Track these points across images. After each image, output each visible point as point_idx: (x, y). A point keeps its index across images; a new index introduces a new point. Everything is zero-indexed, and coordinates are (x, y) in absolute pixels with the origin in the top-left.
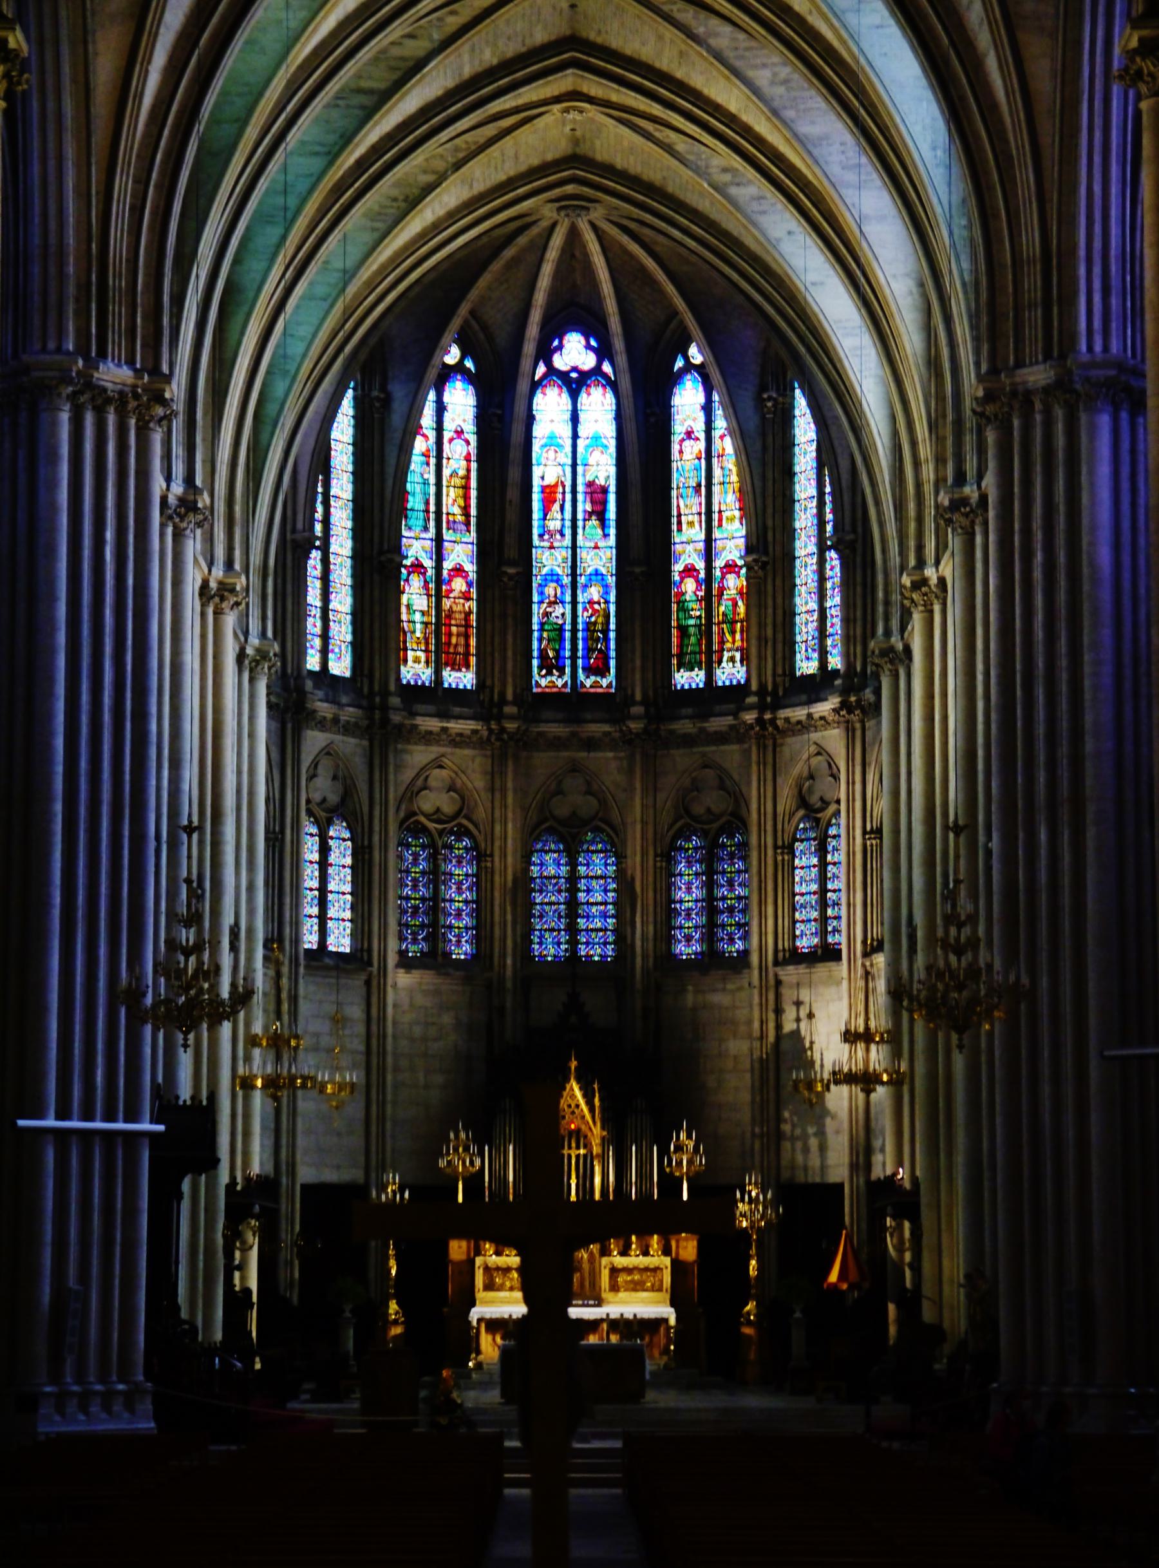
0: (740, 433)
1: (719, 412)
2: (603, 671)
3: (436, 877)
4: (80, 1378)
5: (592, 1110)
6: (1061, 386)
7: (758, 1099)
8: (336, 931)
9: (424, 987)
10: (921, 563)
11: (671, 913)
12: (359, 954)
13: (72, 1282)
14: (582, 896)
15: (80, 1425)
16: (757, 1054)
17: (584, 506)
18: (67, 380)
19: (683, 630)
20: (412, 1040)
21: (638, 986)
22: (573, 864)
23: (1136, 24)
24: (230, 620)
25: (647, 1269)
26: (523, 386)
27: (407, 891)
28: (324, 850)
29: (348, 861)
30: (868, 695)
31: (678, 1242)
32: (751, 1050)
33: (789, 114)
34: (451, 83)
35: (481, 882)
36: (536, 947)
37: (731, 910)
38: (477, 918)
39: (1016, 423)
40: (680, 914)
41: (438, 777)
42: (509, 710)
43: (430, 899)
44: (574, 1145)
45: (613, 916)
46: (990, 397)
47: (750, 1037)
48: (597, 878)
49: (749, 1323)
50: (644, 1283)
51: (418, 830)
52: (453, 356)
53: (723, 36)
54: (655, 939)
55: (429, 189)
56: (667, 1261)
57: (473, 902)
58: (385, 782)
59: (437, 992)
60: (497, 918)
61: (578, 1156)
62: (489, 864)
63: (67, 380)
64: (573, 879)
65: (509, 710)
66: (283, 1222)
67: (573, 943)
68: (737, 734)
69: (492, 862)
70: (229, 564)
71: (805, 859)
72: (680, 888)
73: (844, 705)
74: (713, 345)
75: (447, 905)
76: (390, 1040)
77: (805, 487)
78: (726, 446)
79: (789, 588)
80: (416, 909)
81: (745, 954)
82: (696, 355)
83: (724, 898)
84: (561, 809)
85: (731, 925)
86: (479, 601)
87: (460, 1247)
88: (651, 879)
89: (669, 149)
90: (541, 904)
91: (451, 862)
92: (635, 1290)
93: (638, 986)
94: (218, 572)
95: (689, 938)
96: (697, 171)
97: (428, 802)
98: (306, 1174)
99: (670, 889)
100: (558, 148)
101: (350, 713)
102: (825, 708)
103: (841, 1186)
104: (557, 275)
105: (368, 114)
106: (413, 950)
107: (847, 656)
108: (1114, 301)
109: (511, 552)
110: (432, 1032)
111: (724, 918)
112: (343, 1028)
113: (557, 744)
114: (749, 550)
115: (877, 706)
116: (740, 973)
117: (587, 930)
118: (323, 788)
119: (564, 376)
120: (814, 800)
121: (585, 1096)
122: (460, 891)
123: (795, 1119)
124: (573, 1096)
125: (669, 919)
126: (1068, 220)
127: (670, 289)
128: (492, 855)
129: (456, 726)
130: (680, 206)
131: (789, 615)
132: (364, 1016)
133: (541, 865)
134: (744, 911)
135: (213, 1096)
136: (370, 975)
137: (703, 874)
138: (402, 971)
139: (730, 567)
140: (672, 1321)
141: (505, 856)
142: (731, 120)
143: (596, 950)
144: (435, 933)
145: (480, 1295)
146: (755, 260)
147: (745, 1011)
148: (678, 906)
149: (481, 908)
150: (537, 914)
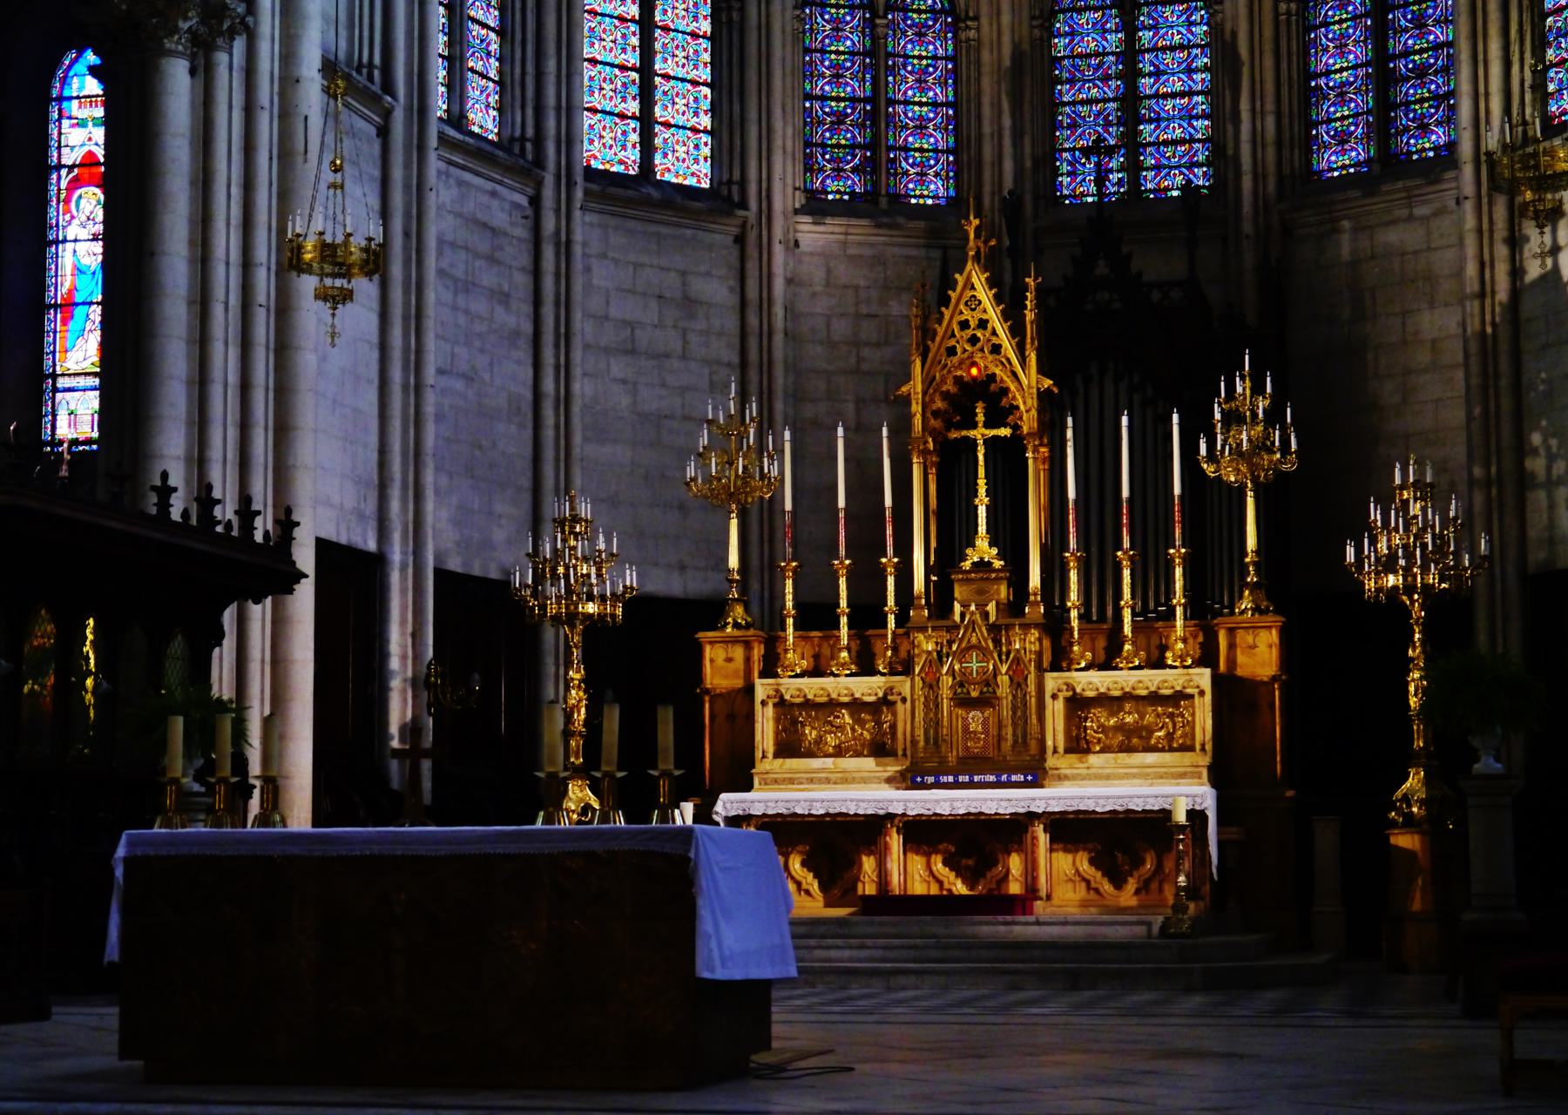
5: (1017, 331)
7: (1477, 411)
8: (681, 149)
9: (851, 251)
12: (725, 192)
14: (1146, 83)
16: (1473, 325)
20: (832, 345)
21: (1247, 227)
22: (1130, 29)
25: (1155, 698)
27: (822, 86)
29: (705, 26)
31: (1231, 632)
32: (1463, 325)
35: (961, 69)
36: (1066, 180)
37: (1421, 72)
38: (957, 133)
40: (1326, 97)
43: (865, 100)
44: (981, 418)
45: (1204, 116)
47: (1461, 303)
48: (1172, 49)
49: (1410, 823)
50: (1151, 732)
54: (1279, 143)
56: (1203, 677)
57: (947, 104)
59: (878, 261)
60: (987, 129)
61: (990, 443)
62: (972, 34)
64: (1130, 54)
66: (549, 661)
69: (978, 29)
72: (1326, 50)
75: (900, 109)
76: (779, 339)
80: (840, 117)
81: (1451, 146)
83: (1407, 53)
85: (1421, 101)
87: (729, 660)
88: (1268, 32)
90: (1073, 103)
91: (904, 33)
92: (1127, 748)
93: (1247, 227)
95: (1342, 138)
99: (1307, 54)
110: (869, 331)
111: (1408, 90)
112: (692, 316)
116: (1438, 181)
117: (1156, 144)
121: (998, 299)
122: (921, 84)
123: (1554, 442)
124: (974, 303)
125: (1307, 106)
128: (976, 18)
132: (734, 300)
133: (1072, 34)
134: (1446, 70)
136: (744, 225)
137: (1366, 15)
138: (808, 219)
141: (999, 14)
145: (767, 764)
147: (1450, 255)
148: (1322, 82)
149: (961, 118)
150: (1066, 121)
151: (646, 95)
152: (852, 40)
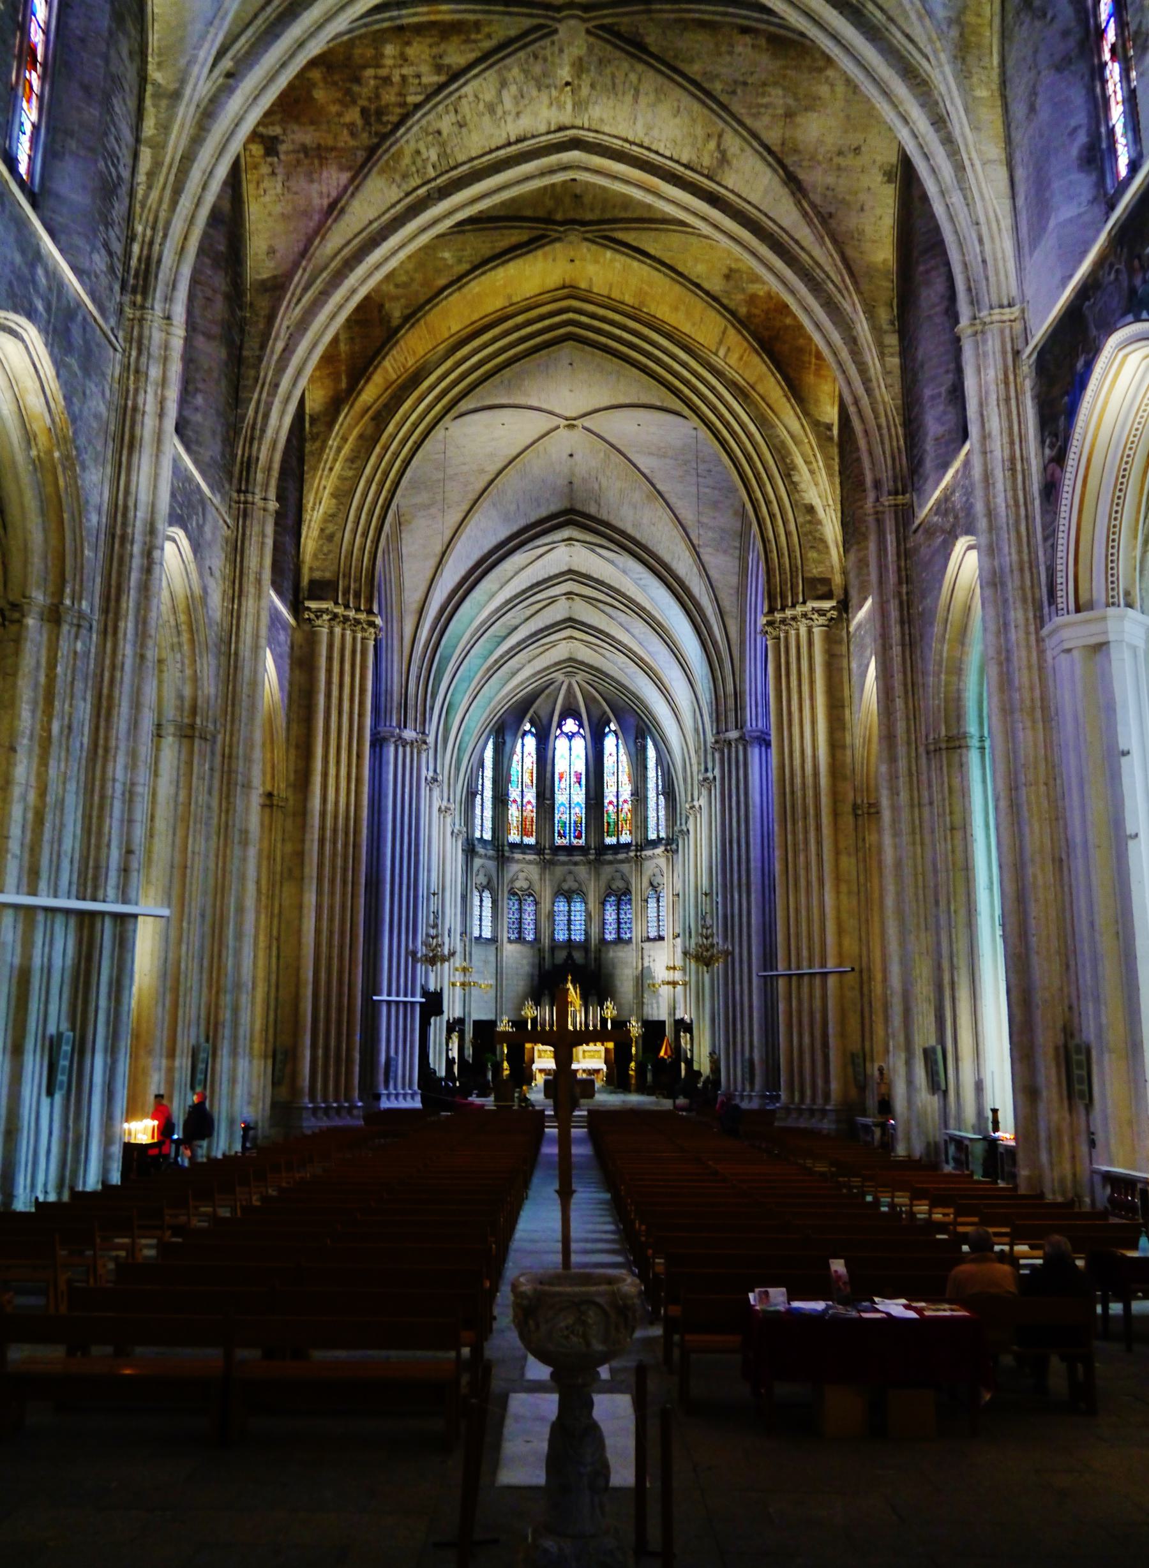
0: (629, 755)
1: (621, 746)
2: (579, 837)
3: (520, 910)
4: (395, 1088)
6: (742, 738)
10: (693, 800)
11: (604, 924)
13: (392, 1053)
15: (394, 1104)
17: (574, 779)
18: (393, 736)
19: (609, 824)
22: (569, 906)
23: (765, 615)
24: (449, 820)
26: (552, 737)
28: (481, 901)
30: (674, 846)
33: (645, 644)
34: (528, 633)
35: (536, 913)
39: (726, 751)
41: (521, 875)
42: (547, 851)
46: (717, 742)
51: (515, 894)
52: (527, 727)
53: (622, 617)
55: (519, 670)
58: (503, 877)
63: (393, 736)
64: (569, 911)
65: (547, 851)
67: (570, 934)
68: (627, 861)
70: (449, 800)
71: (652, 904)
73: (666, 850)
74: (619, 723)
77: (651, 773)
78: (624, 758)
79: (646, 809)
82: (613, 726)
84: (566, 886)
86: (537, 813)
89: (604, 656)
94: (445, 803)
96: (612, 662)
97: (518, 884)
98: (476, 1016)
100: (565, 656)
101: (491, 853)
102: (660, 850)
103: (664, 1022)
104: (565, 698)
105: (499, 644)
106: (513, 937)
107: (667, 833)
108: (759, 709)
109: (548, 795)
113: (564, 864)
114: (632, 795)
115: (677, 850)
118: (481, 879)
119: (567, 734)
120: (655, 884)
126: (742, 681)
127: (604, 704)
129: (528, 857)
130: (607, 675)
131: (646, 818)
135: (441, 989)
139: (625, 801)
140: (604, 1067)
142: (625, 646)
143: (578, 937)
144: (520, 931)
145: (536, 1059)
146: (633, 694)
149: (536, 922)
151: (481, 920)
152: (516, 906)
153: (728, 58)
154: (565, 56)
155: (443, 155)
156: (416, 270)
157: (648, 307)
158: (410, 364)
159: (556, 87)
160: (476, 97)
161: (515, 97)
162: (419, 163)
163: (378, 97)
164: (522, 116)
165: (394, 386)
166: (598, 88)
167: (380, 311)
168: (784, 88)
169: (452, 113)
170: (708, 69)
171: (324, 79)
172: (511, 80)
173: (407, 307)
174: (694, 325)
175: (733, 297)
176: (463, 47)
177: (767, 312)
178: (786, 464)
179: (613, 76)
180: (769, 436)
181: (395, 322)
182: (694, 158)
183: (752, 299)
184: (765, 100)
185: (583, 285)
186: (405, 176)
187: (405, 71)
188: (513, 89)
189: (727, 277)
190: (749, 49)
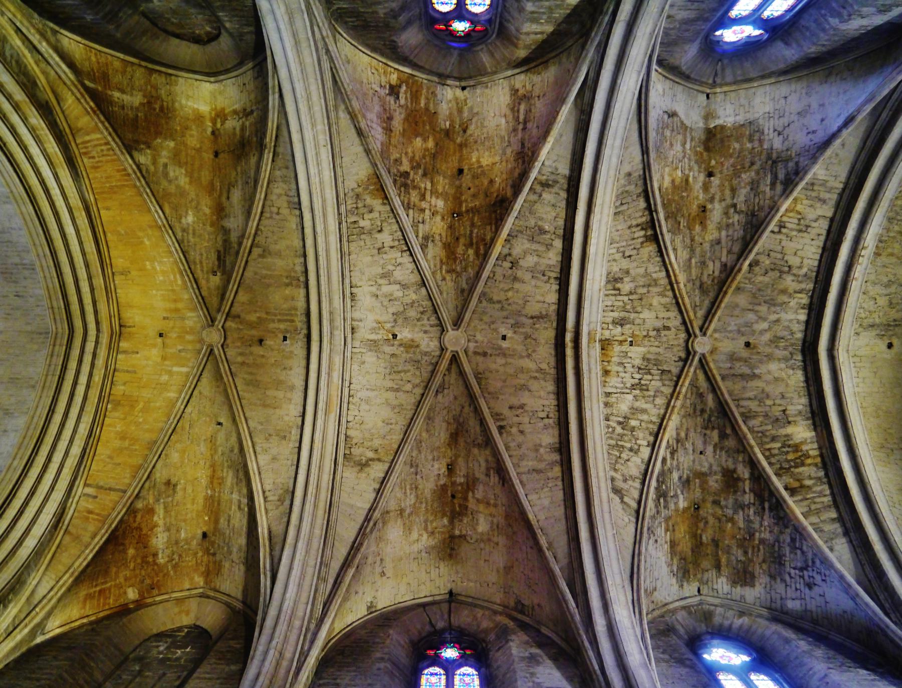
153: (430, 457)
154: (421, 335)
155: (362, 231)
156: (178, 187)
157: (114, 409)
158: (85, 160)
159: (393, 327)
160: (400, 264)
161: (391, 295)
162: (362, 210)
163: (415, 187)
164: (374, 299)
165: (71, 137)
166: (392, 360)
167: (145, 143)
168: (415, 504)
169: (392, 244)
170: (423, 444)
171: (427, 150)
172: (406, 293)
173: (147, 171)
174: (110, 457)
175: (151, 492)
176: (438, 258)
177: (139, 529)
178: (9, 594)
179: (406, 372)
180: (29, 565)
181: (136, 154)
182: (355, 441)
183: (151, 511)
184: (408, 491)
185: (124, 345)
186: (358, 196)
187: (427, 212)
188: (400, 294)
189: (168, 483)
190: (436, 473)
